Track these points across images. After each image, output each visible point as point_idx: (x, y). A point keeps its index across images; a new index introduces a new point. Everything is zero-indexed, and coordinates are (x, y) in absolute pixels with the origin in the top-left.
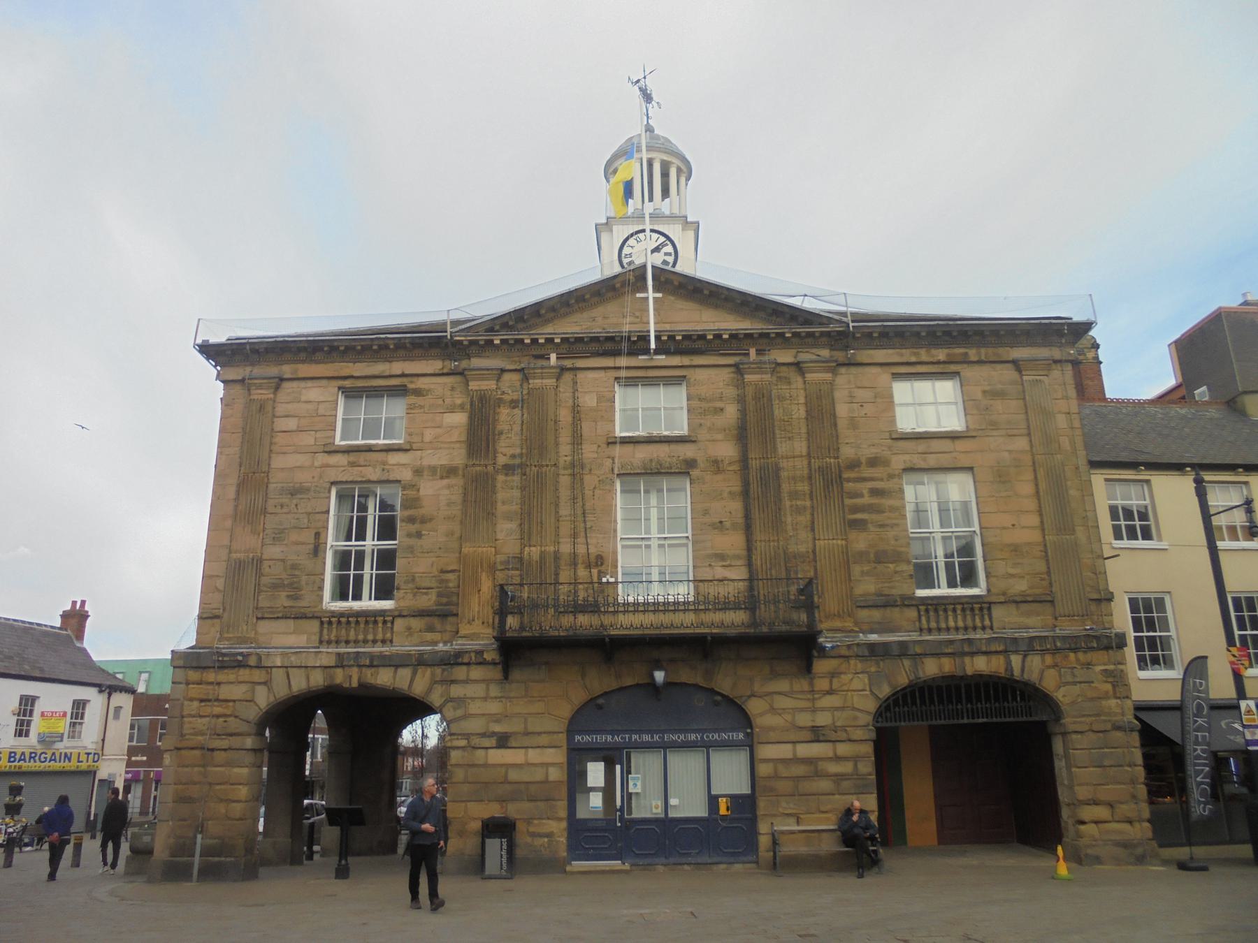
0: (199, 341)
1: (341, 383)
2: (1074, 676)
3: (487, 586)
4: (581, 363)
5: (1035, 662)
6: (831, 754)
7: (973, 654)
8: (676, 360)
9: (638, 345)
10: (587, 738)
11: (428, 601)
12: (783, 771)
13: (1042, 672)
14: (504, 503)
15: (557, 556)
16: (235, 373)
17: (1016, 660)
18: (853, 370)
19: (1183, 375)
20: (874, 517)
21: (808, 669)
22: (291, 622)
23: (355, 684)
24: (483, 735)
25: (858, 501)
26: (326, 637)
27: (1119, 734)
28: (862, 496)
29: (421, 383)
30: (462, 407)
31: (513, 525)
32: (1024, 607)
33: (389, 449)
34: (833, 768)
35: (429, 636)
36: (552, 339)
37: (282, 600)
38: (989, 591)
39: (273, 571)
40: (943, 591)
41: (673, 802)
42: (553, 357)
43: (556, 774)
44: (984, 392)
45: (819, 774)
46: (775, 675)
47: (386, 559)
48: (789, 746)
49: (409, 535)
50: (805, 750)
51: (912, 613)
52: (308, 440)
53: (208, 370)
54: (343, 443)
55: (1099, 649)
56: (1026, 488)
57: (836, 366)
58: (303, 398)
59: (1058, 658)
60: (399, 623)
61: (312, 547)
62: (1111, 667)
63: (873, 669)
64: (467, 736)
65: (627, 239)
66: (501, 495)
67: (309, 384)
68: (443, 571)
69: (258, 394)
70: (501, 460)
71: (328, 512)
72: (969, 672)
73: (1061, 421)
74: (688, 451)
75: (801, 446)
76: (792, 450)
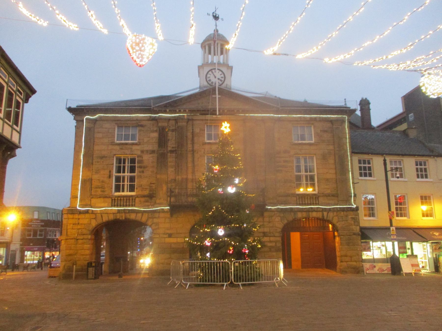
0: (68, 107)
1: (116, 122)
2: (342, 219)
3: (165, 188)
6: (269, 240)
7: (312, 211)
11: (146, 192)
13: (333, 217)
14: (170, 162)
15: (187, 179)
19: (406, 109)
23: (124, 218)
24: (164, 234)
27: (354, 236)
30: (156, 131)
31: (173, 169)
32: (329, 197)
33: (133, 144)
34: (269, 244)
37: (99, 192)
38: (318, 192)
44: (321, 131)
47: (132, 179)
49: (140, 172)
52: (106, 140)
53: (70, 117)
54: (118, 142)
56: (331, 161)
61: (108, 175)
62: (353, 216)
63: (282, 215)
64: (159, 234)
66: (169, 160)
67: (105, 122)
68: (151, 183)
70: (169, 149)
71: (113, 164)
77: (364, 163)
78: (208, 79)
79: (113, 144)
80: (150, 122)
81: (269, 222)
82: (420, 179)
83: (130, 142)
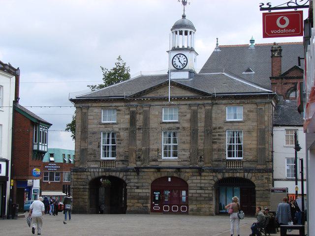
3: (134, 155)
5: (250, 175)
9: (166, 99)
11: (122, 158)
13: (252, 177)
16: (78, 105)
17: (246, 174)
18: (217, 105)
20: (219, 141)
24: (134, 186)
25: (215, 137)
28: (216, 136)
29: (120, 108)
33: (113, 124)
34: (204, 195)
39: (90, 152)
40: (235, 158)
43: (149, 195)
45: (201, 196)
48: (195, 191)
49: (118, 143)
50: (199, 191)
53: (72, 104)
57: (212, 105)
58: (94, 111)
59: (256, 174)
69: (84, 111)
70: (137, 127)
74: (178, 125)
75: (203, 124)
76: (201, 125)
78: (174, 63)
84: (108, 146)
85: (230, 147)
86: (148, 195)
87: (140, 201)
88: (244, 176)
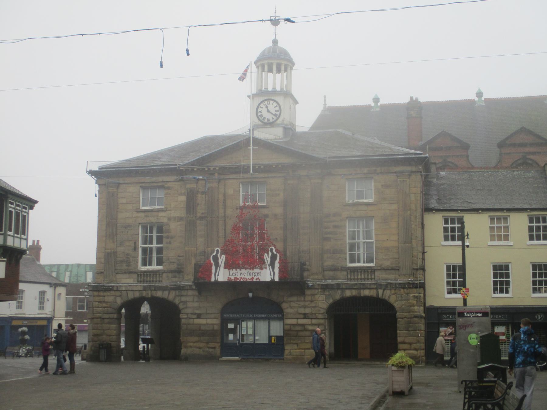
0: (88, 170)
2: (402, 297)
4: (227, 177)
5: (388, 292)
6: (310, 323)
7: (364, 289)
8: (262, 175)
9: (246, 170)
10: (227, 315)
11: (174, 267)
12: (293, 328)
13: (389, 296)
17: (380, 292)
21: (303, 294)
22: (127, 274)
26: (139, 279)
29: (169, 185)
32: (388, 272)
33: (159, 211)
34: (311, 328)
35: (174, 279)
36: (215, 168)
37: (124, 267)
40: (362, 264)
41: (257, 338)
42: (216, 174)
44: (382, 186)
45: (305, 330)
46: (292, 295)
48: (295, 320)
49: (167, 243)
50: (301, 321)
51: (345, 273)
53: (92, 180)
54: (143, 208)
55: (412, 288)
59: (397, 291)
60: (164, 275)
62: (417, 295)
63: (327, 293)
64: (187, 314)
65: (259, 104)
68: (179, 256)
71: (139, 234)
72: (362, 295)
73: (413, 197)
77: (453, 222)
78: (259, 114)
79: (139, 211)
80: (177, 183)
81: (312, 301)
82: (535, 242)
83: (156, 207)
84: (151, 249)
85: (352, 247)
86: (216, 327)
87: (202, 338)
88: (378, 294)
